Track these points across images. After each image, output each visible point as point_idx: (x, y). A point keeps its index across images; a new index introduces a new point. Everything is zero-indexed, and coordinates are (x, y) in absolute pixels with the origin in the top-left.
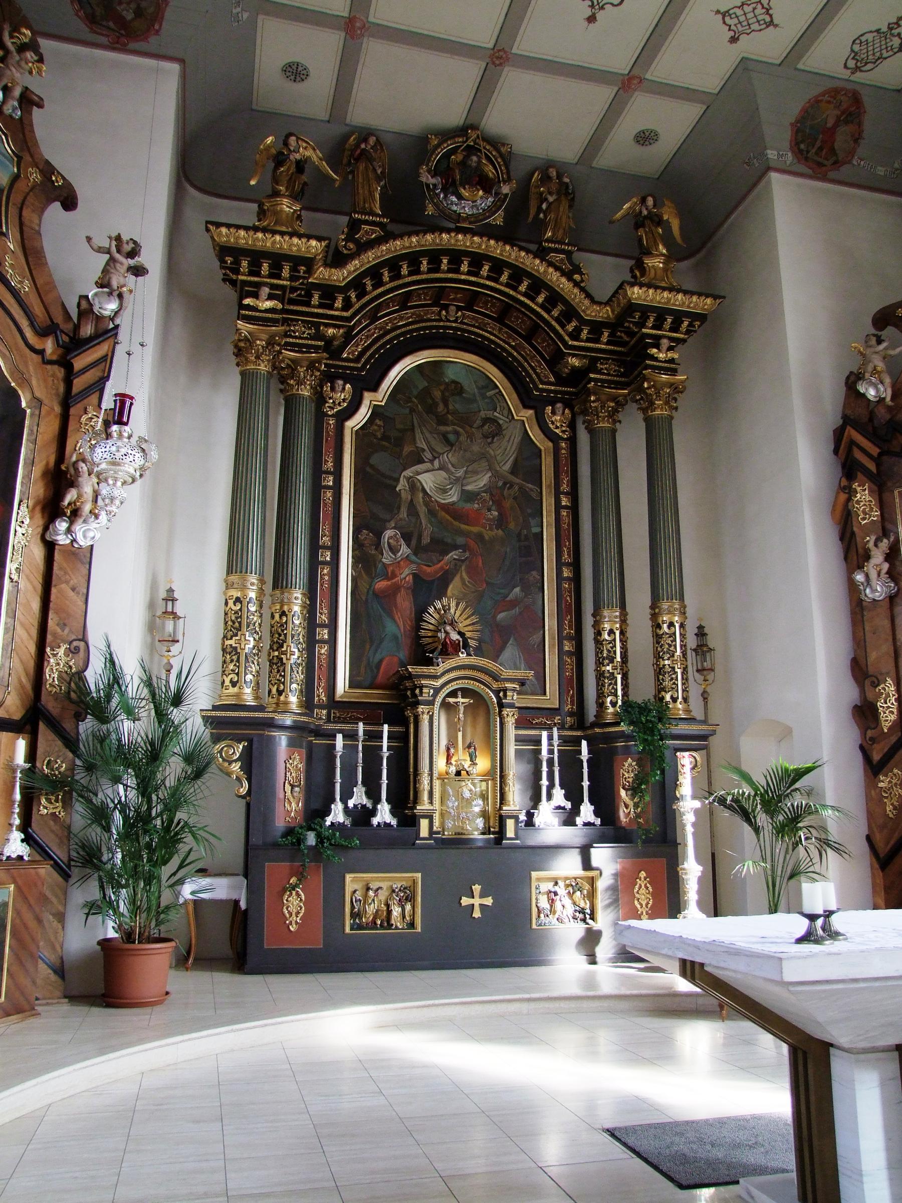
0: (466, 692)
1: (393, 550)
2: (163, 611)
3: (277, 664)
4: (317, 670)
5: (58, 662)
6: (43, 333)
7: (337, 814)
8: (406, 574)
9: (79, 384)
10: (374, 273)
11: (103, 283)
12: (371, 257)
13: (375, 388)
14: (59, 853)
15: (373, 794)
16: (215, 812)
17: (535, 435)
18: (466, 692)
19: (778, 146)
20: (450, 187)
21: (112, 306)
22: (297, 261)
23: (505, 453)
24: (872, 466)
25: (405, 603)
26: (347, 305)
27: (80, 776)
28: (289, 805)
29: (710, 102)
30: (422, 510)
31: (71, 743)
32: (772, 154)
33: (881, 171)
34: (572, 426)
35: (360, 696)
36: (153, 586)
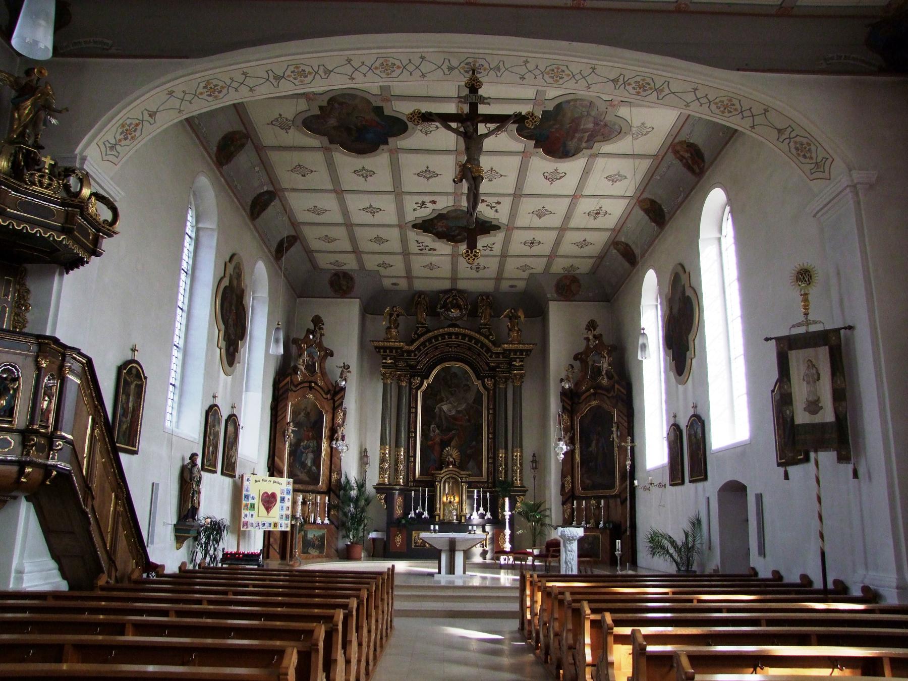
0: (453, 478)
1: (434, 432)
2: (363, 457)
3: (396, 470)
4: (410, 470)
5: (335, 476)
6: (326, 394)
7: (412, 514)
8: (438, 439)
9: (336, 404)
10: (423, 344)
11: (341, 377)
12: (422, 339)
13: (427, 378)
14: (336, 524)
15: (424, 509)
16: (375, 513)
17: (481, 389)
18: (453, 478)
19: (550, 293)
20: (448, 310)
21: (344, 383)
22: (397, 348)
23: (471, 397)
24: (569, 408)
25: (437, 448)
26: (415, 355)
27: (340, 504)
28: (399, 512)
29: (528, 280)
30: (443, 418)
31: (338, 496)
32: (549, 296)
33: (591, 294)
34: (495, 385)
35: (425, 478)
36: (361, 447)
